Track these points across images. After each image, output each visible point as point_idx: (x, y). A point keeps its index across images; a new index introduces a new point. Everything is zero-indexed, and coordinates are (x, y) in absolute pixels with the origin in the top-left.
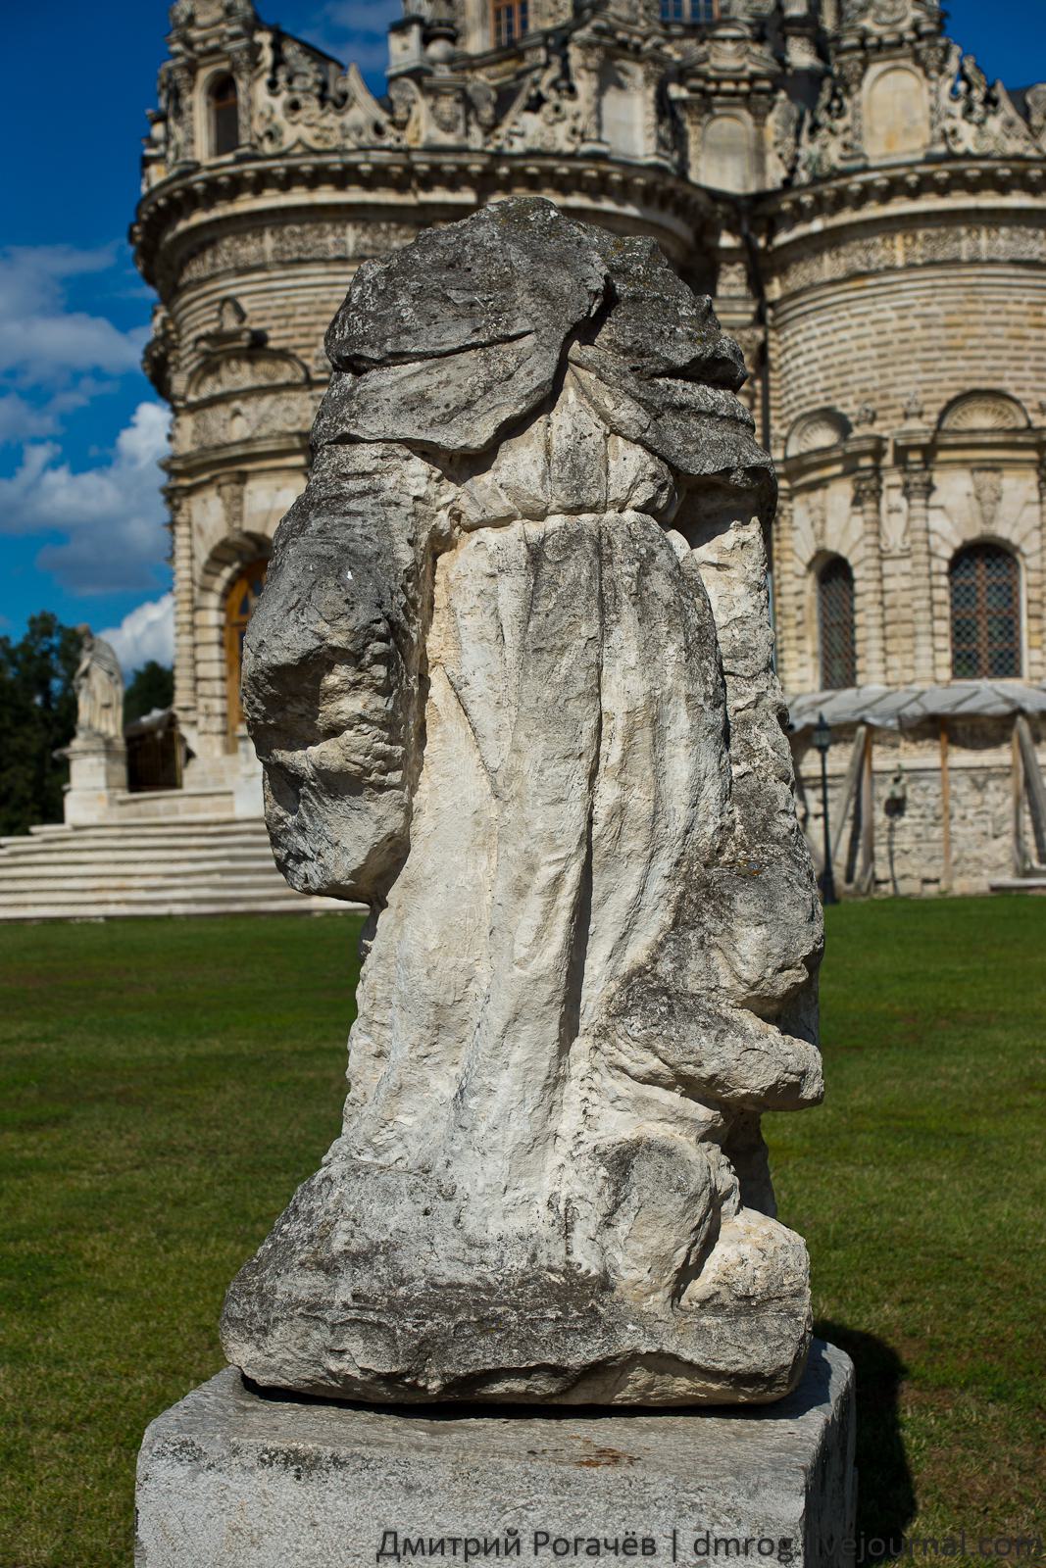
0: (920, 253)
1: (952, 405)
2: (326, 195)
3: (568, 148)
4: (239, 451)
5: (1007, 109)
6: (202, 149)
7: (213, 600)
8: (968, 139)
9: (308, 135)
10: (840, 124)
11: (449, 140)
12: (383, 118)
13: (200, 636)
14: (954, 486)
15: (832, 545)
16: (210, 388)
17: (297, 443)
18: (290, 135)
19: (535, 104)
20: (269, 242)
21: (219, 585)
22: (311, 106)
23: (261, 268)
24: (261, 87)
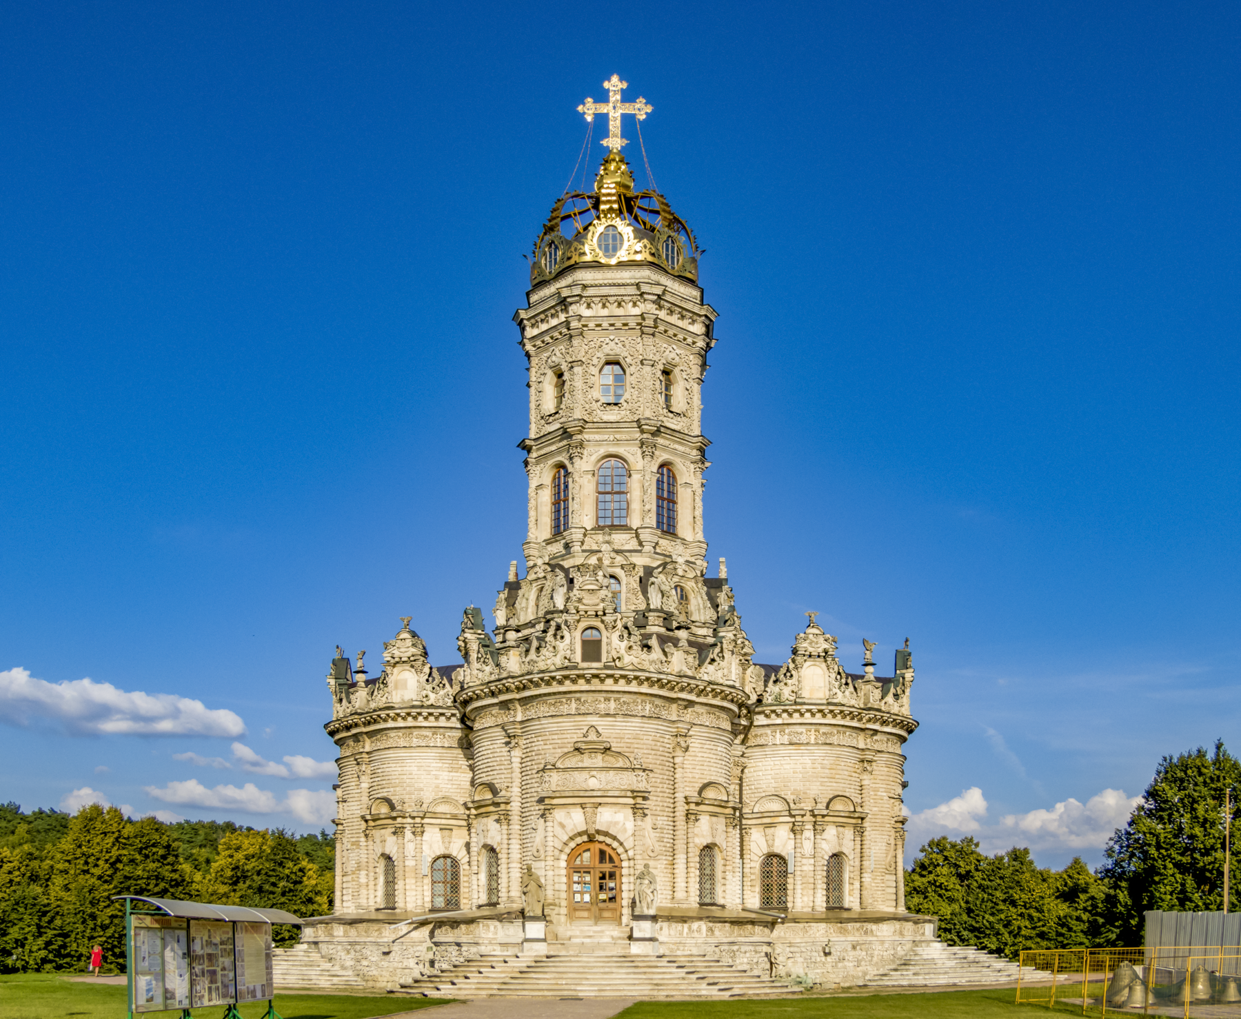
0: (822, 740)
1: (831, 800)
2: (645, 689)
3: (721, 681)
4: (599, 794)
5: (851, 688)
6: (578, 657)
7: (564, 857)
8: (840, 698)
9: (635, 661)
10: (789, 682)
11: (690, 673)
12: (664, 659)
13: (557, 872)
14: (831, 831)
15: (777, 850)
16: (570, 763)
17: (629, 794)
18: (627, 659)
19: (713, 660)
20: (612, 705)
21: (568, 850)
22: (637, 648)
23: (614, 715)
24: (615, 636)
